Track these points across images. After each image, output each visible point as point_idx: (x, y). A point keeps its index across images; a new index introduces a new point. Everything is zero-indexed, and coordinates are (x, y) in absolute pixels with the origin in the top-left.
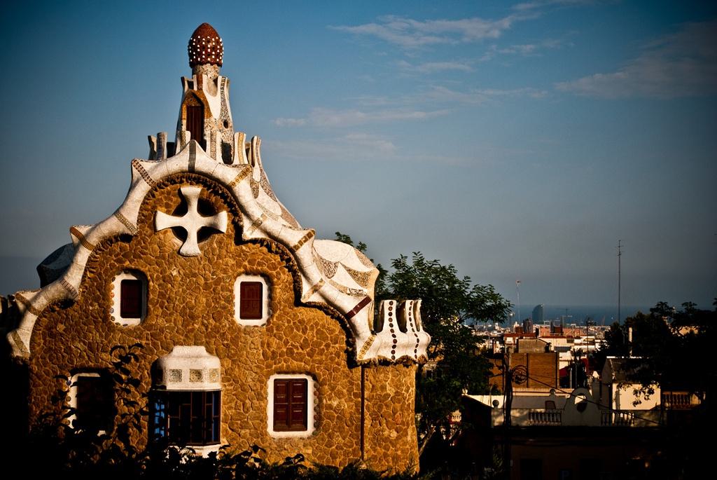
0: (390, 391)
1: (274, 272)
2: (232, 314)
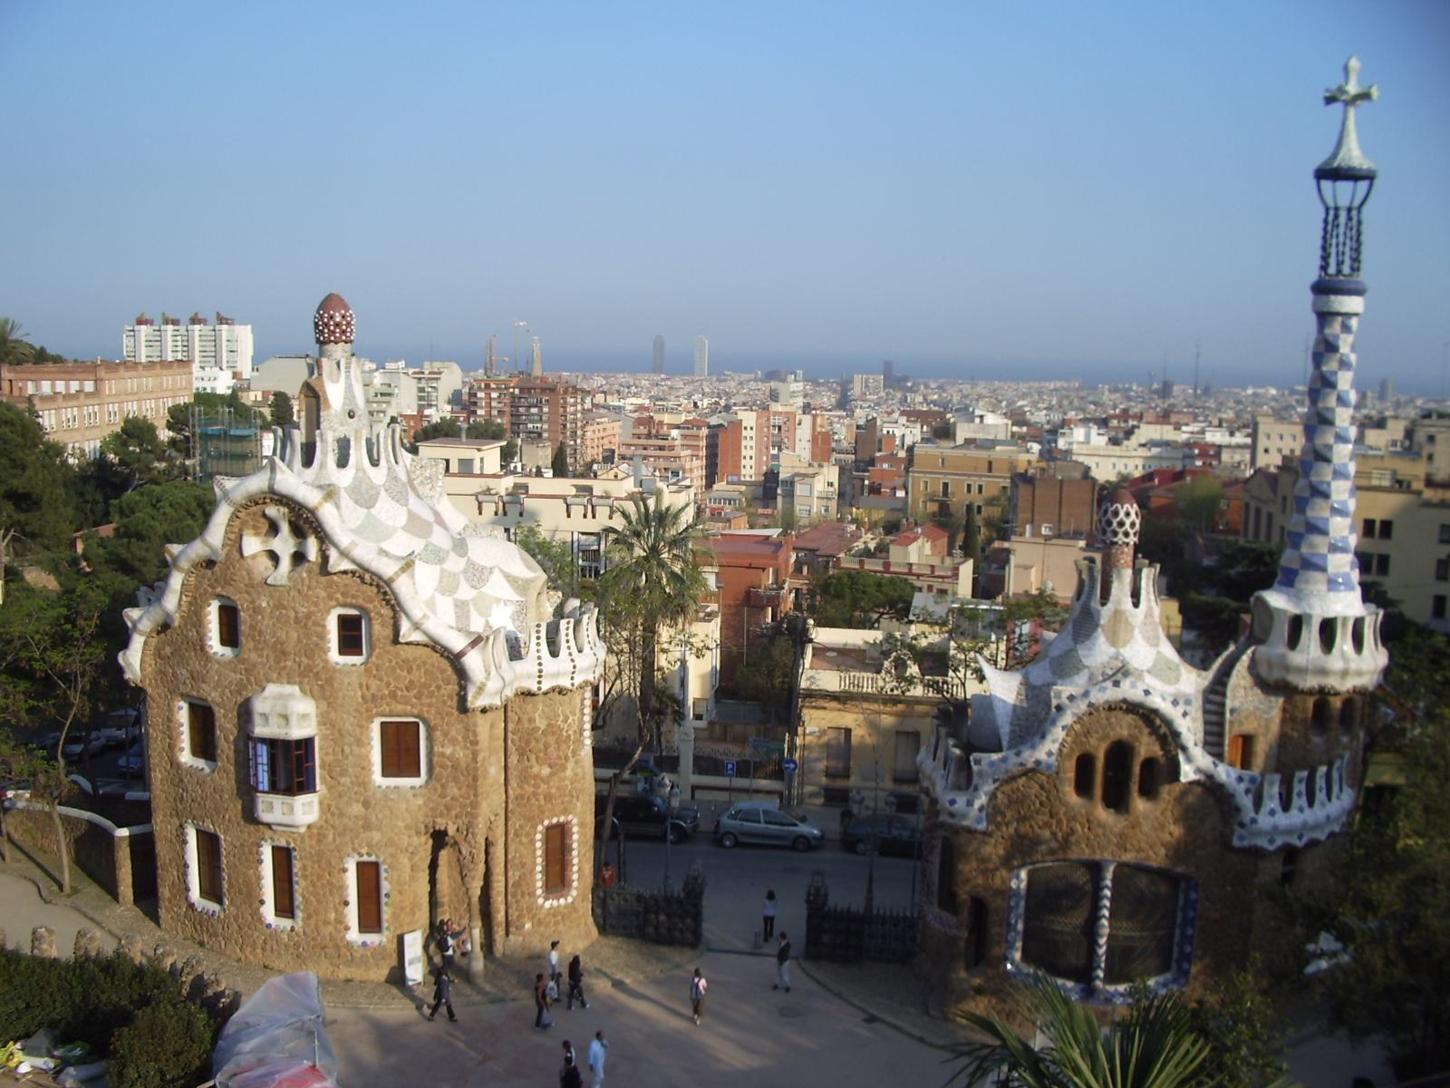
0: (541, 723)
1: (371, 606)
2: (326, 651)
